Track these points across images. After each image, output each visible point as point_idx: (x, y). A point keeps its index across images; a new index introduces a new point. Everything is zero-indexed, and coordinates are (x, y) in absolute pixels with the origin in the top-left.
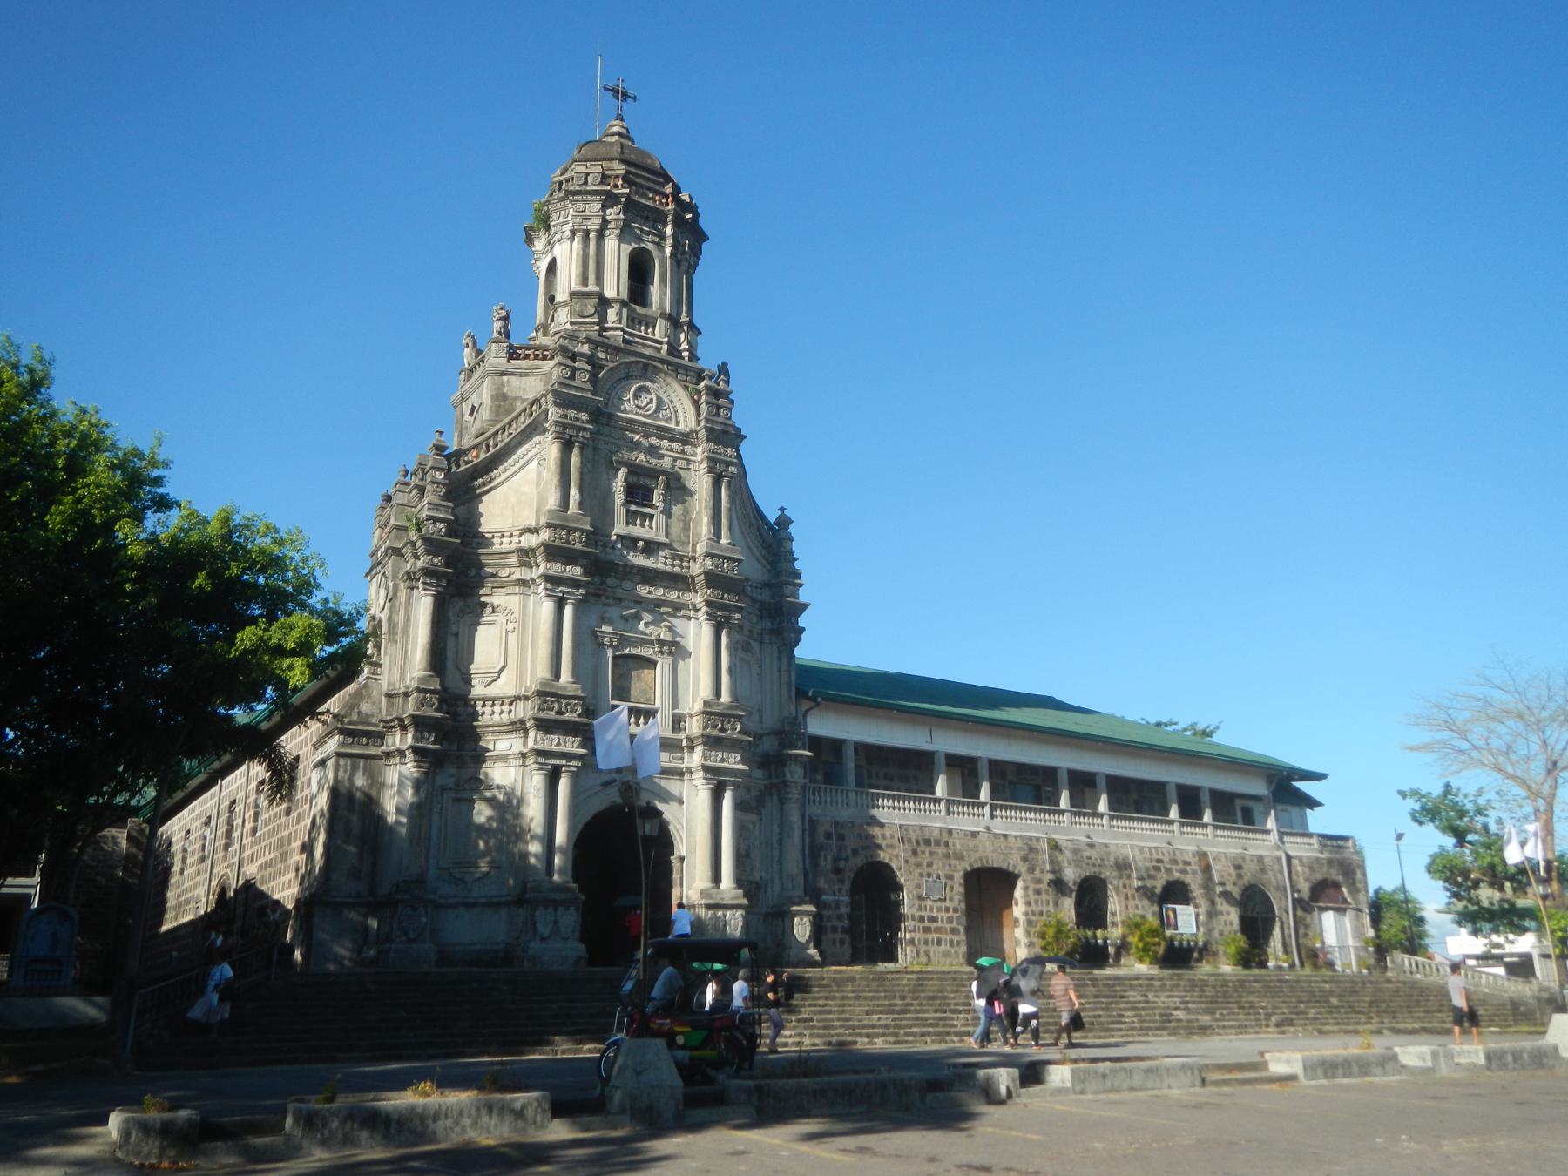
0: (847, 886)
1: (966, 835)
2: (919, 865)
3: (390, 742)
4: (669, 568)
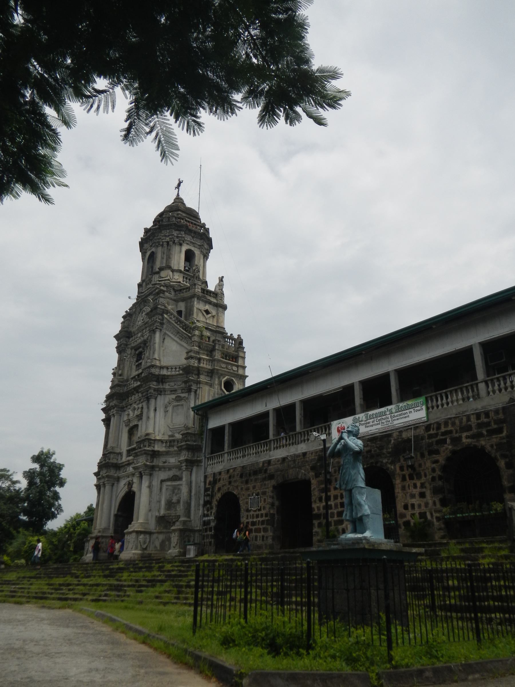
1: (278, 461)
2: (247, 489)
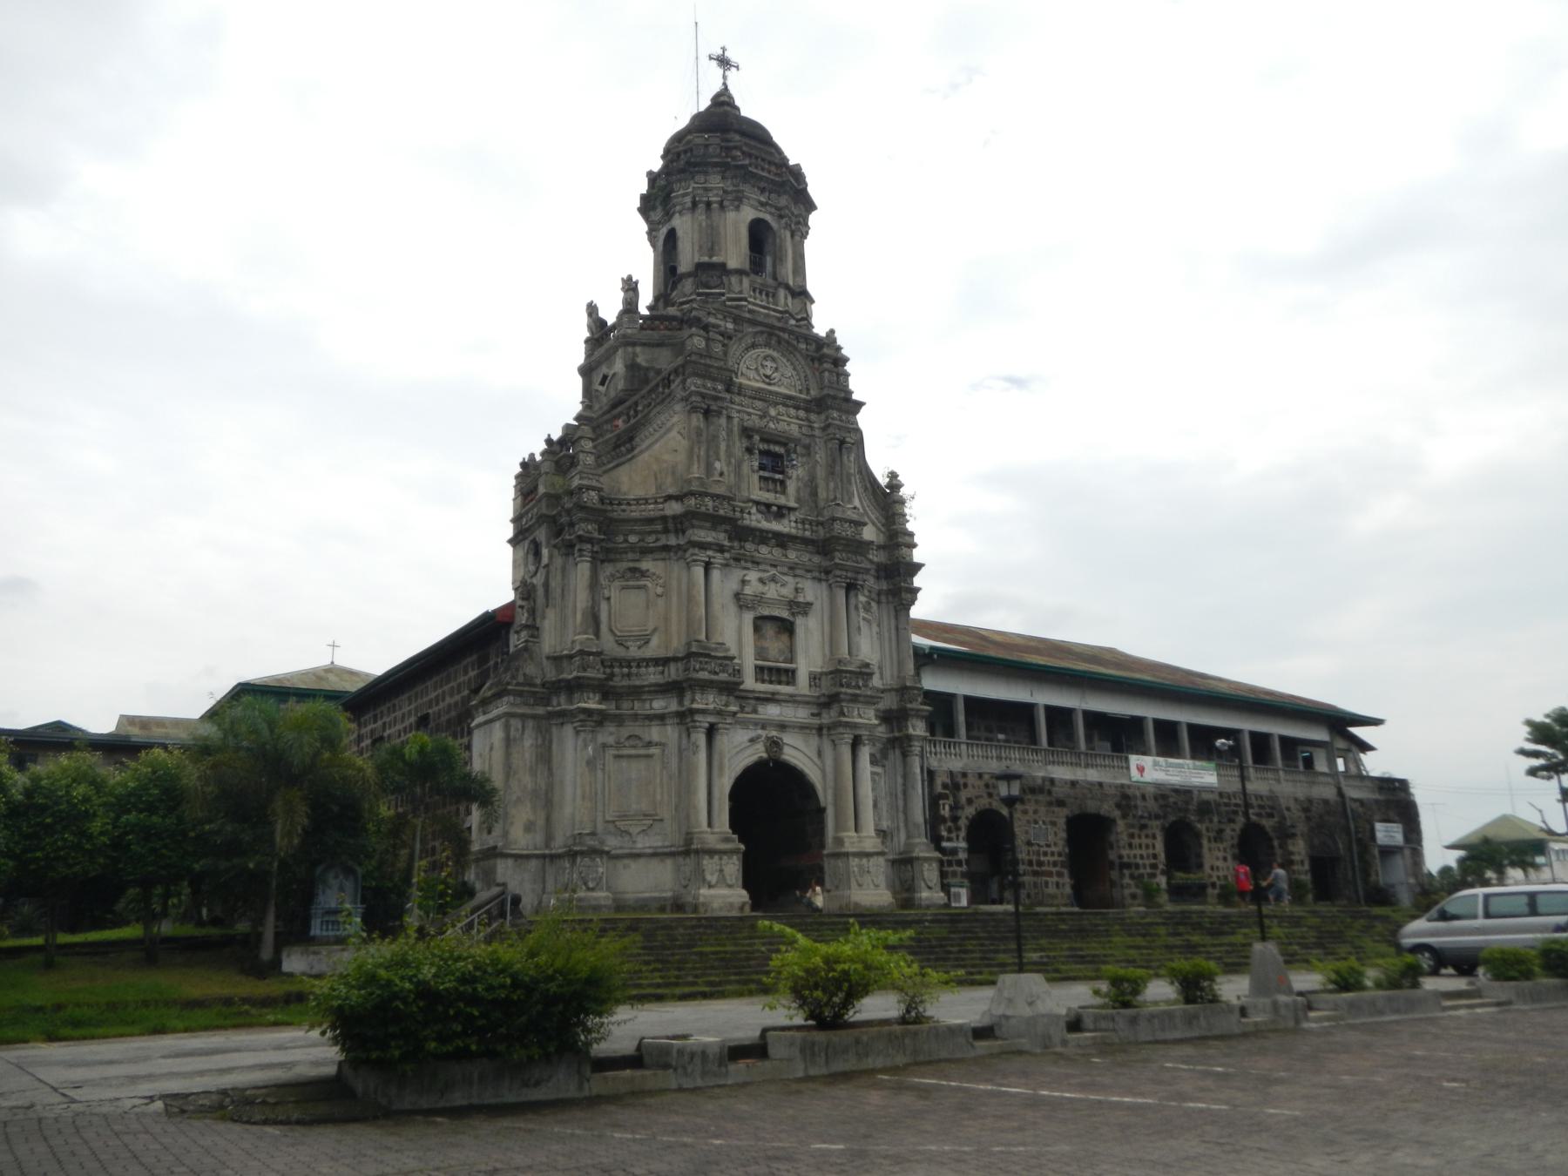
0: (963, 834)
3: (555, 703)
4: (800, 533)
